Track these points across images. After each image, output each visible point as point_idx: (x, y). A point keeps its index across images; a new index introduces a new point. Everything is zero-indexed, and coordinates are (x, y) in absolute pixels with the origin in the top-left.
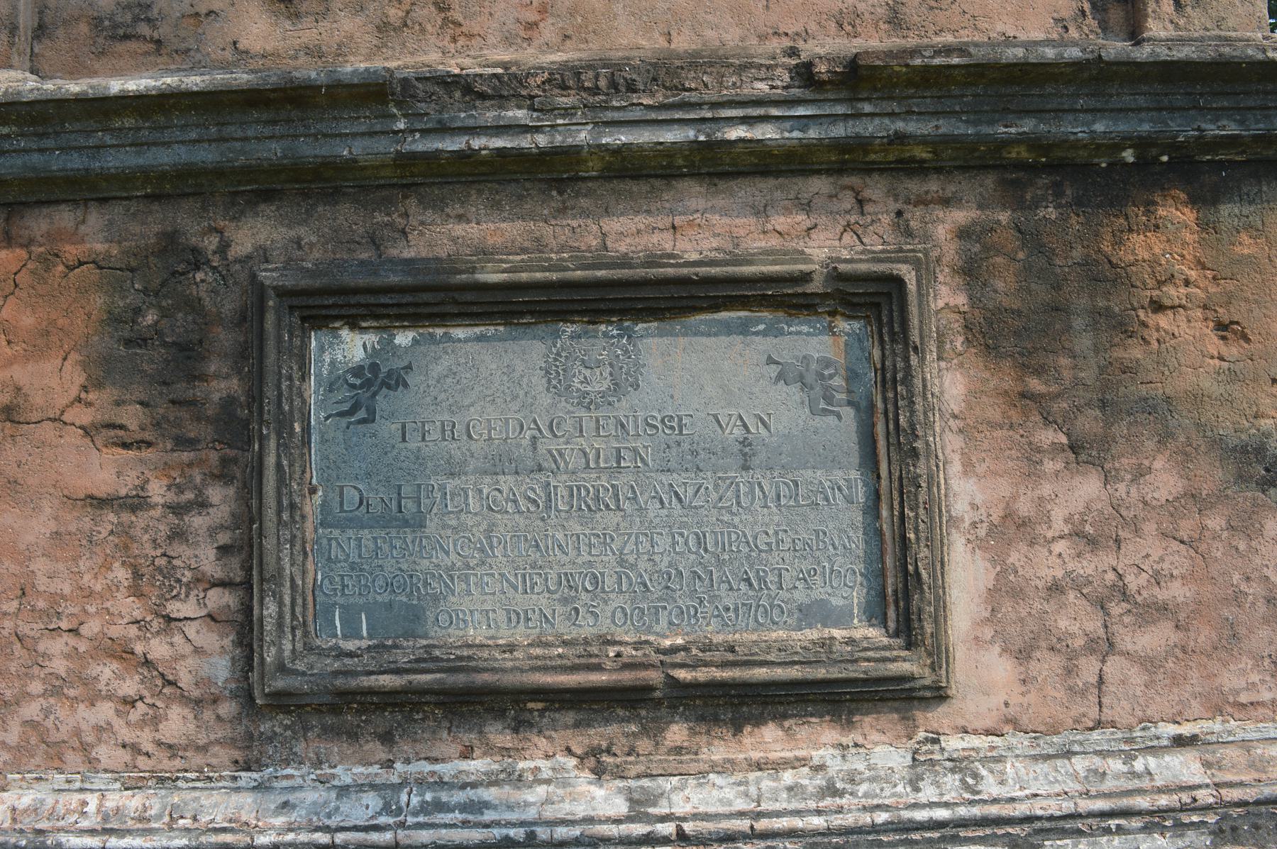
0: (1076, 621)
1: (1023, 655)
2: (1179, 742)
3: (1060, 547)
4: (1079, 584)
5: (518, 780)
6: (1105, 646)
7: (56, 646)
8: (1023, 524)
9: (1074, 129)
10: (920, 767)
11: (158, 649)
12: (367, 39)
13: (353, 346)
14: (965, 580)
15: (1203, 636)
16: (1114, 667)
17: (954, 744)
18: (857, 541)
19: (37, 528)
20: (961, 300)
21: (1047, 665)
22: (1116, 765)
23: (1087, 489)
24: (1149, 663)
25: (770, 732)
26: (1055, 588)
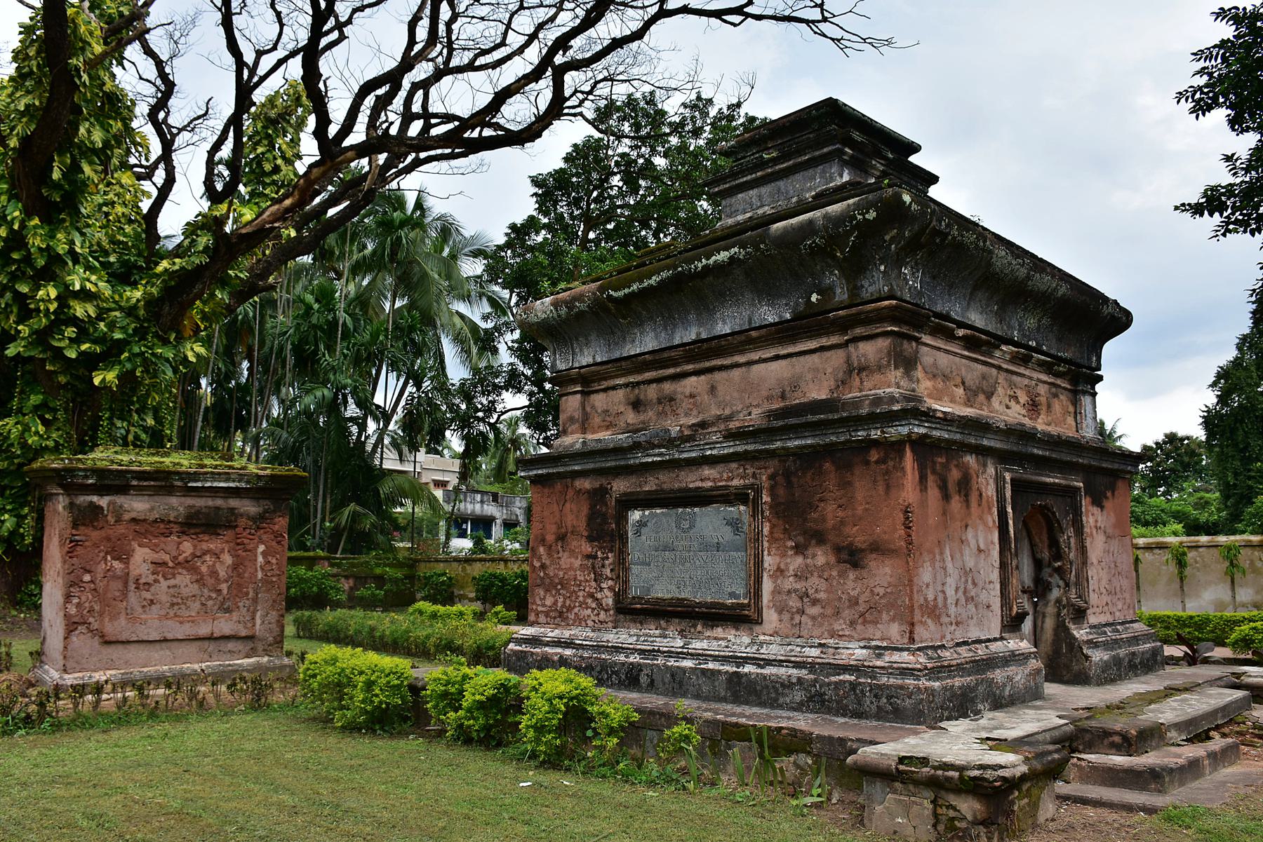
0: (794, 603)
1: (780, 612)
2: (821, 645)
3: (791, 579)
4: (796, 591)
5: (665, 637)
6: (802, 612)
7: (581, 594)
8: (782, 571)
9: (790, 444)
10: (753, 643)
11: (599, 596)
12: (654, 418)
13: (635, 515)
14: (767, 586)
15: (829, 611)
16: (804, 619)
17: (762, 638)
18: (743, 575)
19: (577, 563)
20: (769, 499)
21: (786, 616)
22: (799, 649)
23: (799, 560)
24: (813, 618)
25: (720, 629)
26: (789, 592)
